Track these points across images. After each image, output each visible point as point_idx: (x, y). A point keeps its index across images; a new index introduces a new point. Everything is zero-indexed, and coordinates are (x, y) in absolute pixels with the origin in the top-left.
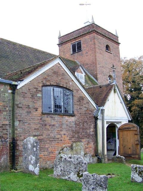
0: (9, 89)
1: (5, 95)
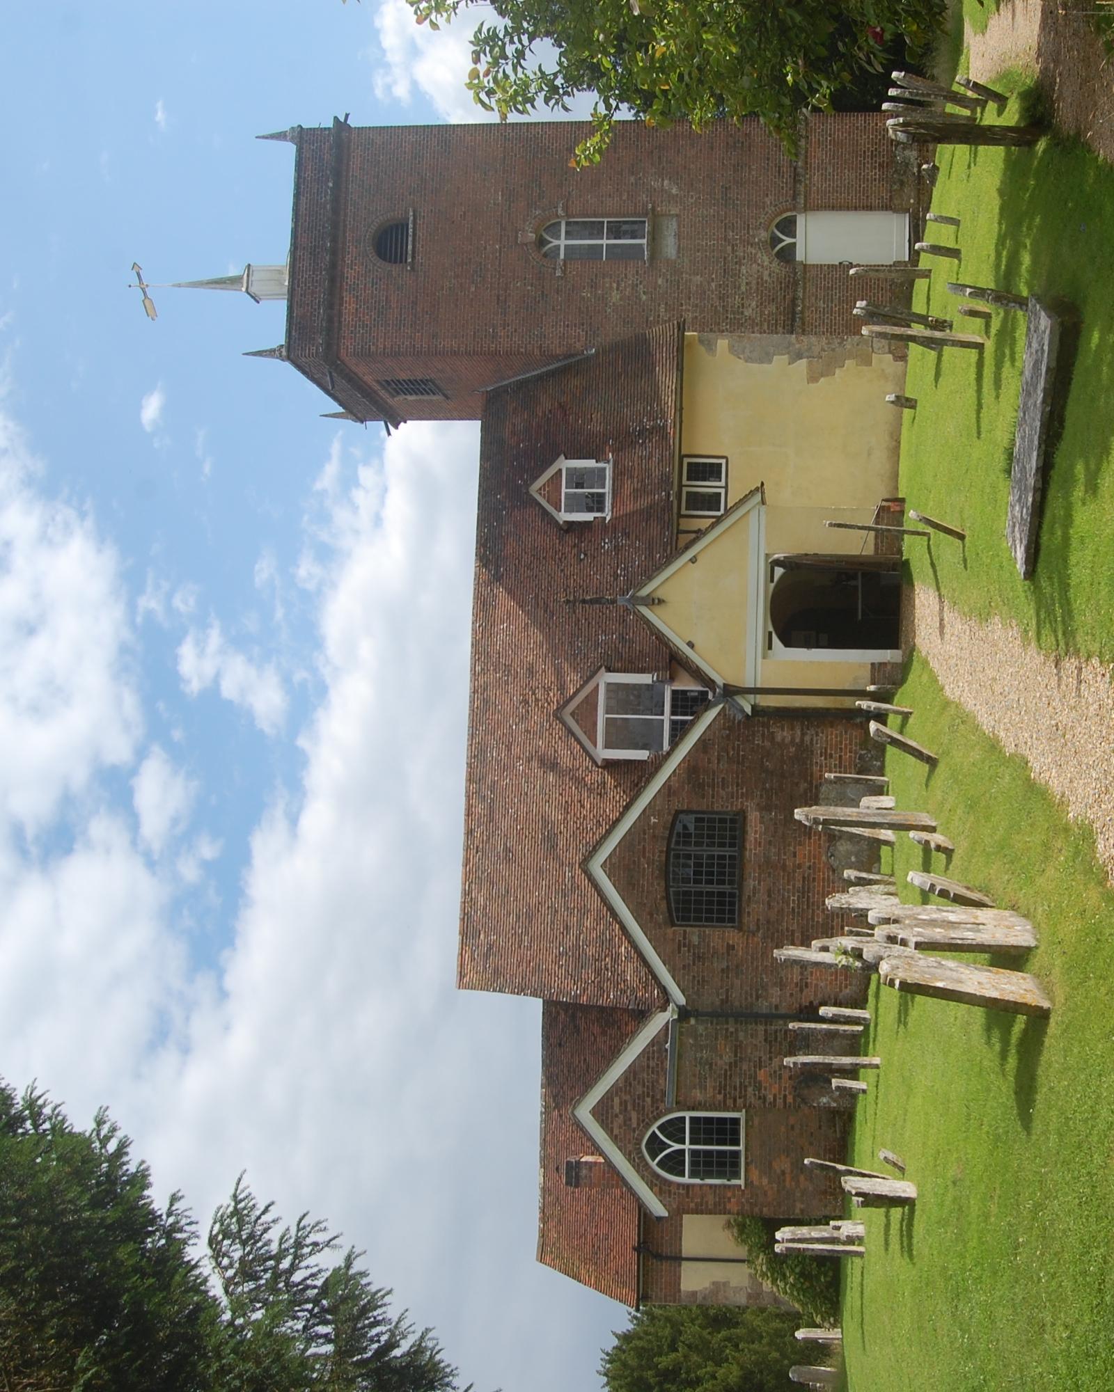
0: (688, 1023)
1: (701, 1035)
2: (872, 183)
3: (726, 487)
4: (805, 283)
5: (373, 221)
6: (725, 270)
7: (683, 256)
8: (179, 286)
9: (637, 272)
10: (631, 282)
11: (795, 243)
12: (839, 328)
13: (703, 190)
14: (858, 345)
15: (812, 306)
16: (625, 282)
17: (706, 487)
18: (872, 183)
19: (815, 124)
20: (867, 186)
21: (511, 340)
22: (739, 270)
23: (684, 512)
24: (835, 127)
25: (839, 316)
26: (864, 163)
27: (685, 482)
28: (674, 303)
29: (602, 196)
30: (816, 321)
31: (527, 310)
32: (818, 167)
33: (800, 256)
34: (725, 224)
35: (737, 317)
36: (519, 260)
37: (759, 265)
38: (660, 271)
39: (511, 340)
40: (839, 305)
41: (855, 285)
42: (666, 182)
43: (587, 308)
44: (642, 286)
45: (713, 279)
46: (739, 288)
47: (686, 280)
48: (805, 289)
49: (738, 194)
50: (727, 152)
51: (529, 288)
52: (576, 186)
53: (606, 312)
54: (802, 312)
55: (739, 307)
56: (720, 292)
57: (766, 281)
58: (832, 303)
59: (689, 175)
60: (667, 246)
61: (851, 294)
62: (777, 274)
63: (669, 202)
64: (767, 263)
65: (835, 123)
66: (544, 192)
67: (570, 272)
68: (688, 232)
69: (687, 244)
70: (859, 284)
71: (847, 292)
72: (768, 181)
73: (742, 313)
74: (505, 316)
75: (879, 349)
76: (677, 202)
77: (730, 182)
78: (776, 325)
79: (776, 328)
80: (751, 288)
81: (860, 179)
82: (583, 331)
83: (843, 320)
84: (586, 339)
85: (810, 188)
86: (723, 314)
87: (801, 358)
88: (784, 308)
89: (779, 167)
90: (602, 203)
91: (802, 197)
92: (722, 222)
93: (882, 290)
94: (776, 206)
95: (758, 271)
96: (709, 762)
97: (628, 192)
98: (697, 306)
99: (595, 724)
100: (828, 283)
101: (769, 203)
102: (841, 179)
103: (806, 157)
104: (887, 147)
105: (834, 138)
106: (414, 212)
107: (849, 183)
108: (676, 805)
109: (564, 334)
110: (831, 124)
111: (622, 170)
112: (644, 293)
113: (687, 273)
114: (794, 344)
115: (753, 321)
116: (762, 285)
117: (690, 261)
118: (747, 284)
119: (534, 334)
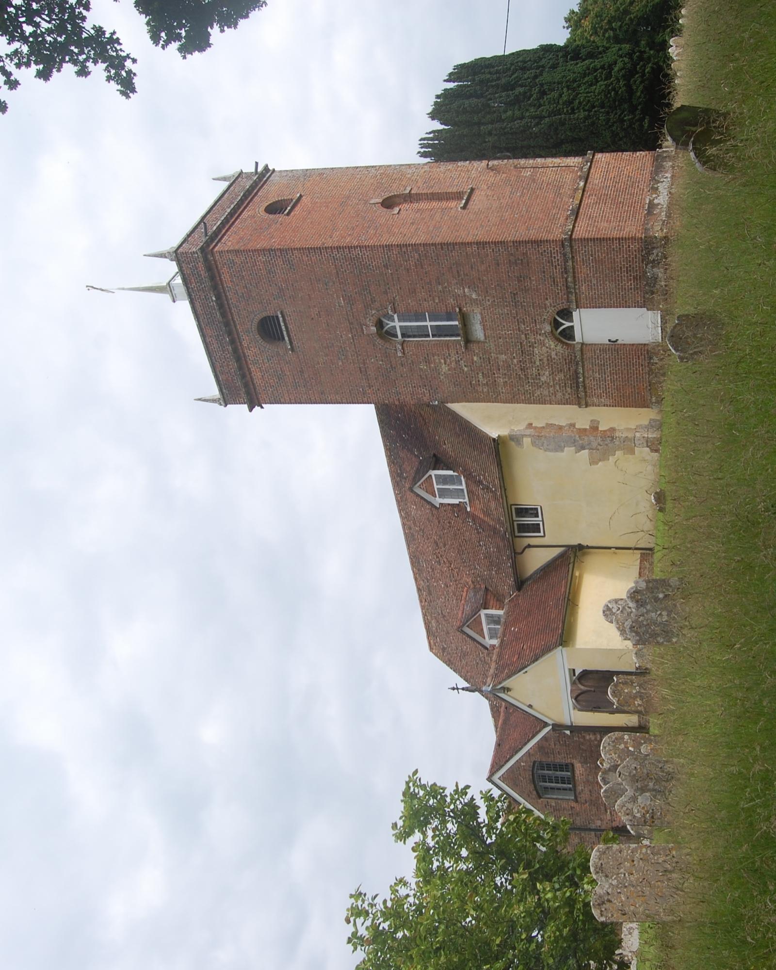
2: (628, 291)
3: (543, 521)
4: (583, 362)
5: (253, 319)
6: (522, 351)
7: (489, 342)
8: (123, 289)
9: (457, 352)
10: (454, 359)
11: (572, 327)
12: (612, 391)
13: (497, 295)
14: (624, 442)
15: (591, 377)
16: (450, 359)
17: (529, 520)
18: (628, 291)
19: (579, 247)
20: (625, 294)
21: (377, 395)
22: (533, 351)
23: (517, 534)
24: (595, 248)
25: (611, 383)
26: (621, 276)
27: (515, 518)
28: (488, 373)
29: (420, 300)
30: (594, 386)
31: (383, 377)
32: (585, 280)
33: (578, 338)
34: (518, 320)
35: (536, 382)
36: (368, 344)
37: (547, 348)
38: (474, 351)
39: (377, 395)
40: (611, 376)
41: (621, 363)
42: (466, 290)
43: (426, 375)
44: (463, 362)
45: (514, 357)
46: (535, 363)
47: (494, 358)
48: (583, 367)
49: (524, 298)
50: (511, 267)
51: (381, 363)
52: (398, 292)
53: (440, 378)
54: (584, 381)
55: (536, 375)
56: (521, 366)
57: (554, 359)
58: (605, 374)
59: (483, 285)
60: (476, 330)
61: (619, 369)
62: (562, 354)
63: (472, 304)
64: (552, 347)
65: (595, 246)
66: (374, 297)
67: (408, 353)
68: (490, 325)
69: (491, 334)
70: (624, 362)
71: (616, 367)
72: (546, 289)
73: (540, 379)
74: (368, 381)
75: (639, 444)
76: (477, 304)
77: (516, 289)
78: (566, 387)
79: (566, 389)
80: (543, 363)
81: (619, 288)
82: (426, 390)
83: (614, 384)
84: (430, 395)
85: (580, 295)
86: (526, 380)
87: (585, 449)
88: (570, 376)
89: (554, 278)
90: (421, 305)
91: (575, 304)
92: (515, 318)
93: (642, 365)
94: (554, 306)
95: (547, 352)
96: (549, 745)
97: (439, 297)
98: (505, 374)
99: (482, 630)
100: (601, 361)
101: (549, 304)
102: (604, 288)
103: (574, 273)
104: (639, 264)
105: (595, 258)
106: (282, 313)
107: (610, 292)
108: (533, 759)
109: (413, 392)
110: (591, 246)
111: (430, 281)
112: (465, 366)
113: (494, 353)
114: (578, 441)
115: (548, 384)
116: (552, 361)
117: (495, 345)
118: (540, 360)
119: (392, 392)
